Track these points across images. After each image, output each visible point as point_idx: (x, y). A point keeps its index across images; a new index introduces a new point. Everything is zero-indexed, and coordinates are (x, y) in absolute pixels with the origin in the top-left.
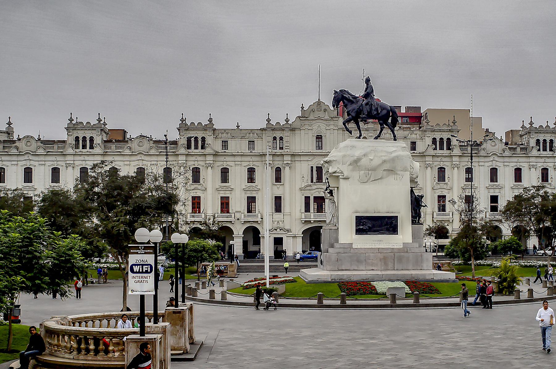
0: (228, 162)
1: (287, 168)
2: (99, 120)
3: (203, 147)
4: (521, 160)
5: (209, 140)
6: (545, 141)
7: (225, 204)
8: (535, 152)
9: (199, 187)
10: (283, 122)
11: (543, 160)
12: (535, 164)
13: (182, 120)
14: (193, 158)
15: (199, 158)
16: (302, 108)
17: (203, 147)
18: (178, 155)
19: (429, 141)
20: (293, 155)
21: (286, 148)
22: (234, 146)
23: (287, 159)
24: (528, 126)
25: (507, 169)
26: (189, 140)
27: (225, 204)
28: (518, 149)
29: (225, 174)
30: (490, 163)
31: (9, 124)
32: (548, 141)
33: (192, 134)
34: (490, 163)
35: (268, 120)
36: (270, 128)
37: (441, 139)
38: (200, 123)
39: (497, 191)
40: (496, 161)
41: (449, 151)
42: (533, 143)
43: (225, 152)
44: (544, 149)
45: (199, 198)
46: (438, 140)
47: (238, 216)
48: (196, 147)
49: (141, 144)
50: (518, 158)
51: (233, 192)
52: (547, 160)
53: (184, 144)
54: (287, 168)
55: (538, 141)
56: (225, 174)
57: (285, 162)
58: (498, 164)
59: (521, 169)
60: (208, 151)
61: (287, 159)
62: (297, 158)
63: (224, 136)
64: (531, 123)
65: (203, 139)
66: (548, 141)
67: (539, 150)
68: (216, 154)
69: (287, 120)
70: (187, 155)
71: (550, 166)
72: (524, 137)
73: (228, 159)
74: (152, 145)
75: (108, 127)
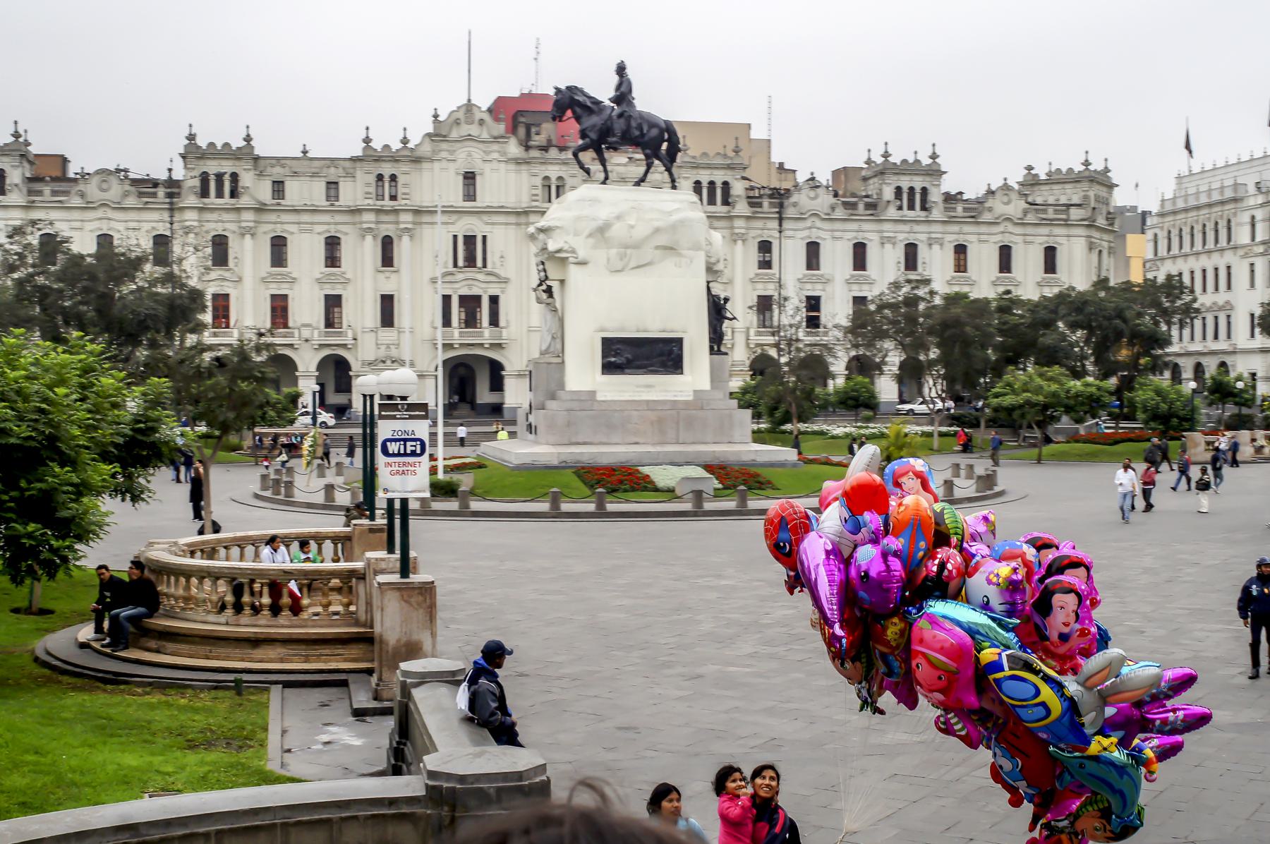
0: (286, 226)
3: (234, 194)
4: (866, 226)
5: (247, 179)
6: (912, 189)
7: (280, 309)
8: (892, 212)
9: (227, 275)
10: (396, 145)
11: (906, 228)
12: (891, 235)
13: (191, 137)
14: (214, 216)
15: (226, 216)
16: (436, 116)
17: (234, 194)
20: (417, 212)
21: (404, 197)
22: (297, 192)
23: (406, 218)
24: (880, 160)
25: (839, 244)
26: (204, 178)
27: (280, 309)
28: (861, 206)
29: (279, 247)
30: (806, 233)
32: (918, 190)
33: (212, 167)
34: (806, 233)
35: (367, 140)
36: (370, 156)
37: (712, 183)
38: (227, 145)
39: (819, 286)
40: (818, 228)
41: (725, 208)
42: (889, 193)
43: (279, 204)
44: (911, 207)
45: (226, 297)
46: (705, 184)
47: (306, 333)
48: (220, 194)
49: (105, 186)
50: (860, 223)
51: (296, 286)
52: (917, 228)
53: (195, 187)
54: (406, 239)
55: (899, 191)
56: (279, 247)
57: (402, 226)
58: (822, 234)
59: (770, 243)
61: (406, 218)
62: (426, 218)
63: (277, 172)
64: (886, 155)
65: (234, 177)
66: (918, 190)
67: (900, 208)
68: (261, 209)
69: (405, 141)
70: (201, 209)
71: (921, 239)
72: (871, 181)
73: (286, 217)
74: (128, 188)
75: (34, 150)
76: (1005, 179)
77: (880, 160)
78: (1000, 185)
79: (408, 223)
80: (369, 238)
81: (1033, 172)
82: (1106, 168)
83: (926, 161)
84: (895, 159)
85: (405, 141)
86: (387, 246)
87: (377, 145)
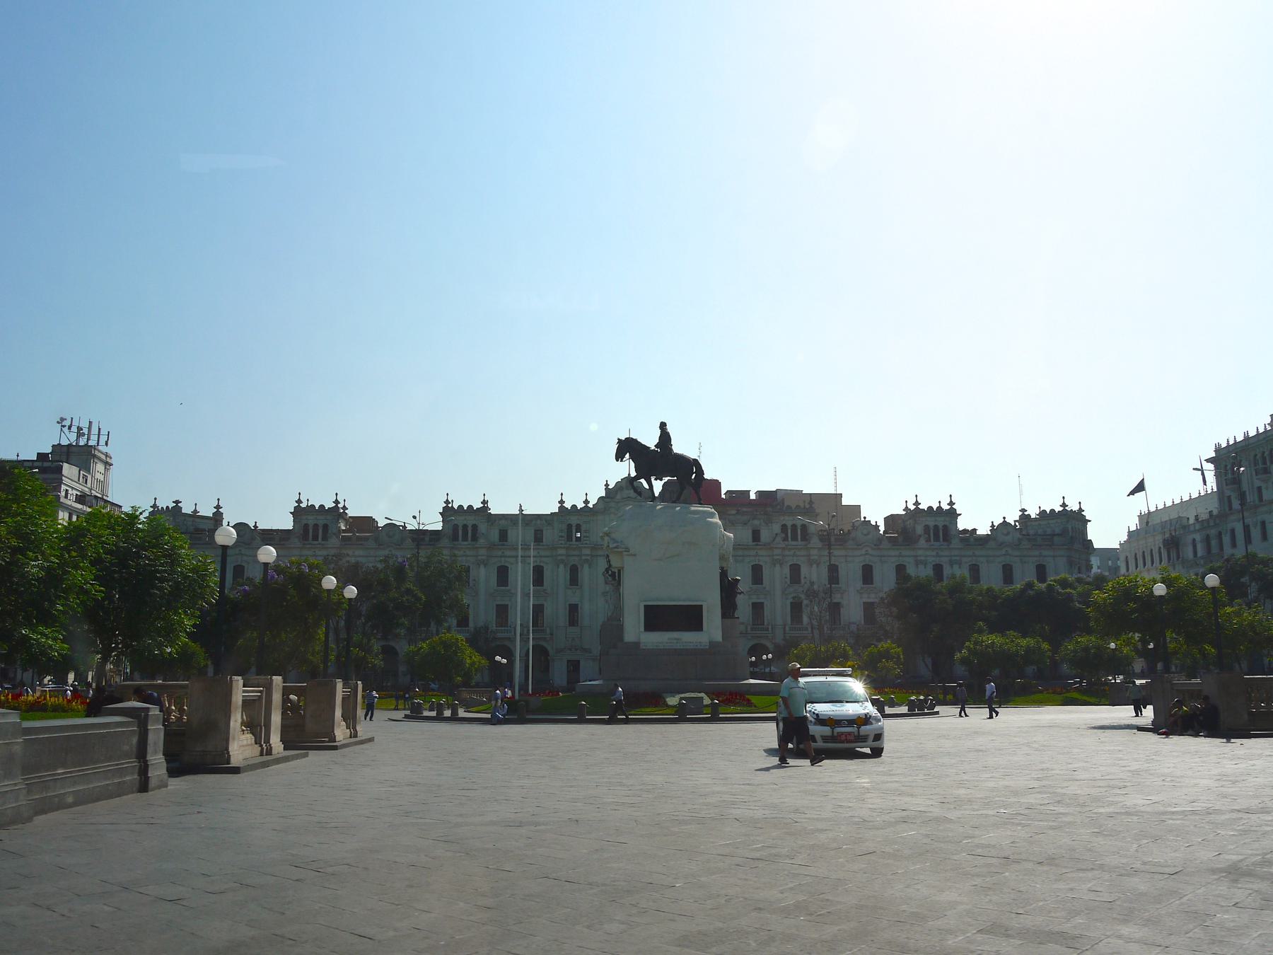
1: (586, 567)
2: (337, 502)
10: (580, 505)
16: (607, 485)
18: (476, 548)
19: (777, 528)
21: (585, 539)
31: (218, 507)
35: (562, 502)
37: (794, 526)
38: (470, 507)
41: (803, 543)
46: (789, 527)
54: (586, 567)
57: (584, 558)
60: (482, 541)
64: (917, 503)
69: (586, 502)
75: (351, 513)
76: (1004, 518)
77: (912, 507)
78: (1001, 522)
79: (588, 555)
80: (562, 566)
81: (1026, 513)
82: (1080, 508)
83: (945, 507)
84: (923, 506)
85: (586, 502)
86: (574, 571)
87: (568, 505)
